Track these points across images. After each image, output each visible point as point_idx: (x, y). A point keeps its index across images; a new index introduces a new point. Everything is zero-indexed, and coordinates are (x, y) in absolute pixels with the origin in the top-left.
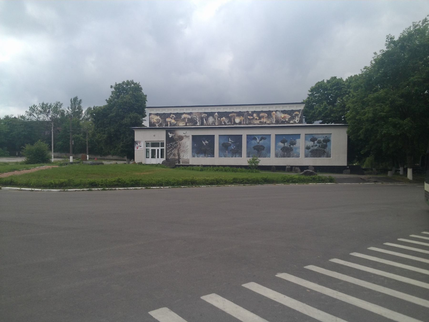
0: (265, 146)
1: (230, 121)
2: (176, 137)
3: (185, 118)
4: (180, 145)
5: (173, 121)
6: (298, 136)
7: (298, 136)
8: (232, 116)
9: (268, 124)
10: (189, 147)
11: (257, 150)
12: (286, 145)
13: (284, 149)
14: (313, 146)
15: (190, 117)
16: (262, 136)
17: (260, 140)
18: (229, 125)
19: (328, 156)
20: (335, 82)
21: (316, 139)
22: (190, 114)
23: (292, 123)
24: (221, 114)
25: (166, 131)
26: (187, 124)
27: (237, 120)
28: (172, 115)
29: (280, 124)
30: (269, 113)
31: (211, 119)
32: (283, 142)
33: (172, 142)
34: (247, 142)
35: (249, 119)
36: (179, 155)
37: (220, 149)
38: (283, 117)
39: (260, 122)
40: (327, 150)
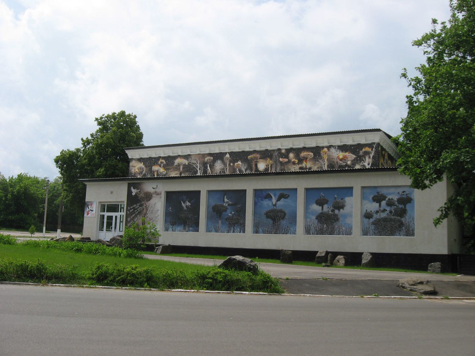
0: (286, 211)
1: (250, 167)
2: (142, 195)
3: (179, 165)
6: (349, 190)
7: (349, 190)
8: (252, 159)
10: (159, 212)
13: (322, 218)
14: (377, 212)
15: (186, 162)
16: (282, 192)
17: (278, 200)
19: (410, 233)
22: (187, 157)
24: (235, 156)
25: (128, 183)
28: (161, 160)
31: (219, 166)
32: (321, 203)
34: (255, 204)
35: (281, 163)
37: (209, 218)
38: (341, 157)
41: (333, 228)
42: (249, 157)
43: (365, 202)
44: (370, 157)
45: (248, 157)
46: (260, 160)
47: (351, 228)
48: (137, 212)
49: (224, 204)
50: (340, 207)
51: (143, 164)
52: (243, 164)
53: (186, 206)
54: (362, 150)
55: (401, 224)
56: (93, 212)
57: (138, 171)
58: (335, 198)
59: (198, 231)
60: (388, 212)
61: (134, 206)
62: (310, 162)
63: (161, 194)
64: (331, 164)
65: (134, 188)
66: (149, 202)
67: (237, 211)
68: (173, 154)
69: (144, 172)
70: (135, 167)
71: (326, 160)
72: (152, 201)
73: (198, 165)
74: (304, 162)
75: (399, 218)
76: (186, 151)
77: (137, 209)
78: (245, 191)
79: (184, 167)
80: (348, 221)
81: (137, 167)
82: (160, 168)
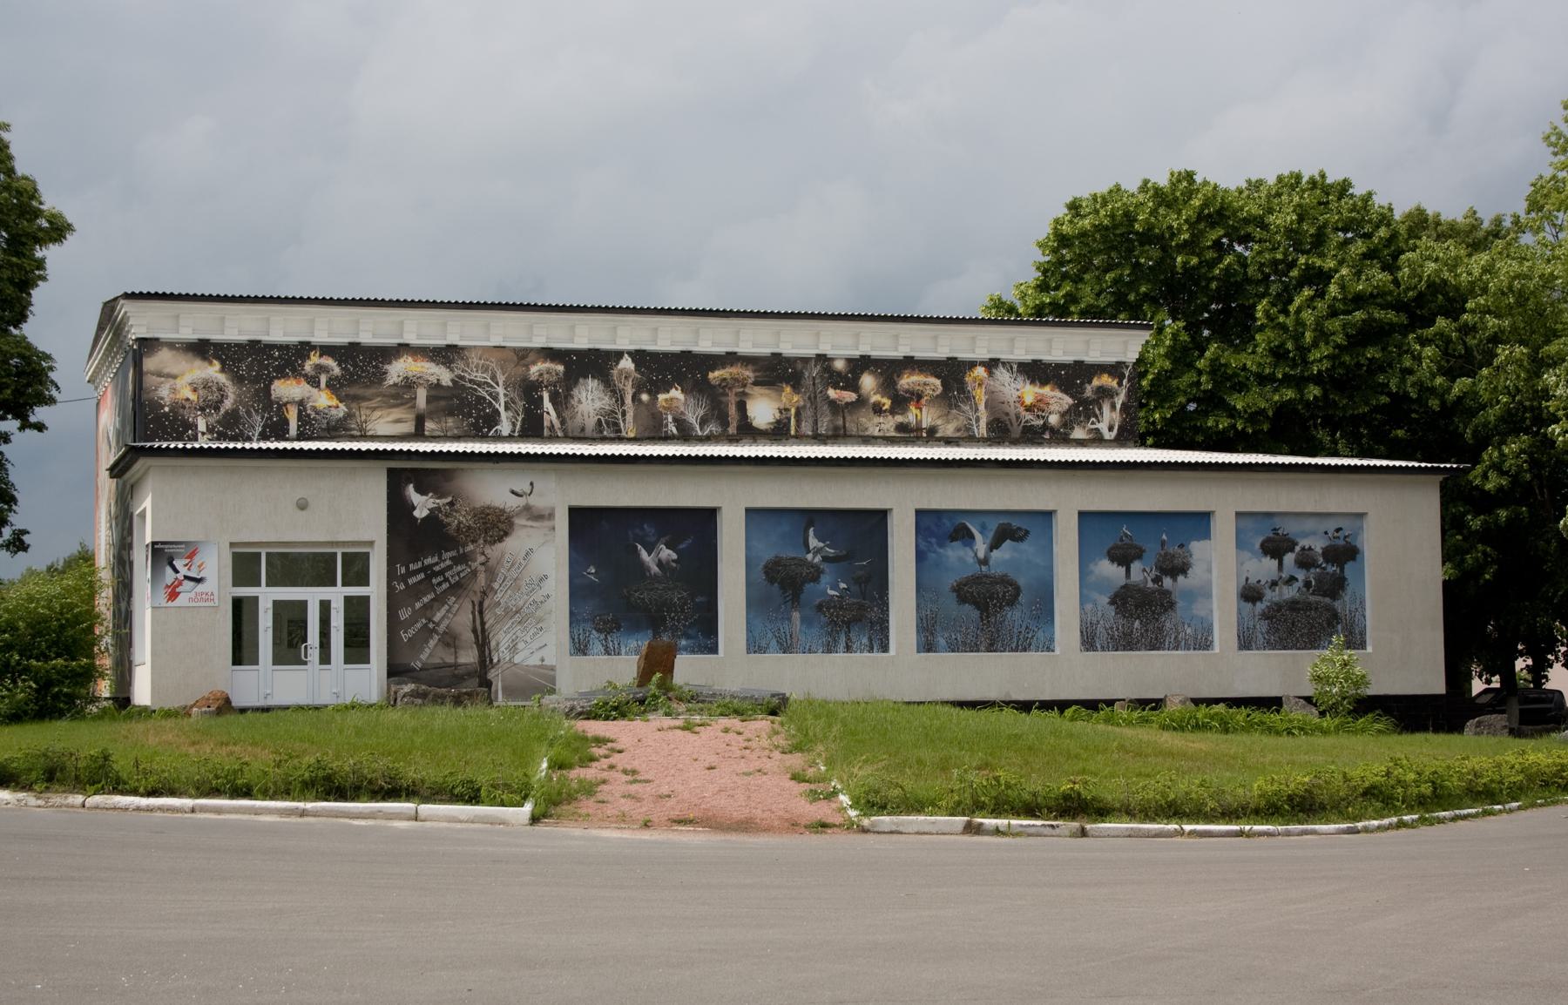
0: (1021, 582)
1: (717, 412)
2: (462, 518)
3: (409, 384)
4: (491, 573)
5: (323, 399)
6: (1199, 522)
7: (1199, 522)
8: (725, 384)
9: (949, 442)
11: (977, 605)
12: (1140, 573)
13: (1125, 599)
14: (1274, 584)
15: (445, 376)
17: (995, 545)
18: (707, 439)
20: (1205, 205)
21: (1291, 546)
22: (446, 354)
23: (1081, 443)
24: (659, 369)
25: (390, 472)
26: (429, 426)
27: (763, 410)
28: (315, 359)
29: (1015, 443)
30: (952, 372)
31: (590, 399)
32: (1123, 557)
33: (435, 544)
34: (920, 556)
35: (833, 405)
36: (483, 641)
37: (756, 603)
38: (1029, 400)
39: (901, 427)
40: (1343, 605)
41: (1161, 630)
42: (714, 376)
43: (1247, 554)
44: (1113, 407)
45: (711, 375)
46: (757, 389)
47: (1210, 630)
48: (445, 586)
49: (809, 557)
50: (1177, 568)
51: (223, 370)
52: (692, 401)
53: (660, 564)
54: (1090, 382)
55: (1334, 618)
56: (200, 588)
57: (193, 397)
58: (1163, 543)
59: (713, 650)
60: (1300, 584)
61: (429, 561)
62: (932, 410)
63: (551, 516)
64: (997, 420)
65: (421, 490)
66: (499, 546)
67: (857, 581)
68: (374, 336)
69: (228, 404)
70: (175, 377)
71: (982, 407)
72: (513, 545)
73: (501, 390)
74: (912, 408)
75: (1327, 600)
77: (442, 572)
78: (881, 516)
79: (433, 393)
80: (1199, 610)
81: (188, 378)
82: (315, 391)
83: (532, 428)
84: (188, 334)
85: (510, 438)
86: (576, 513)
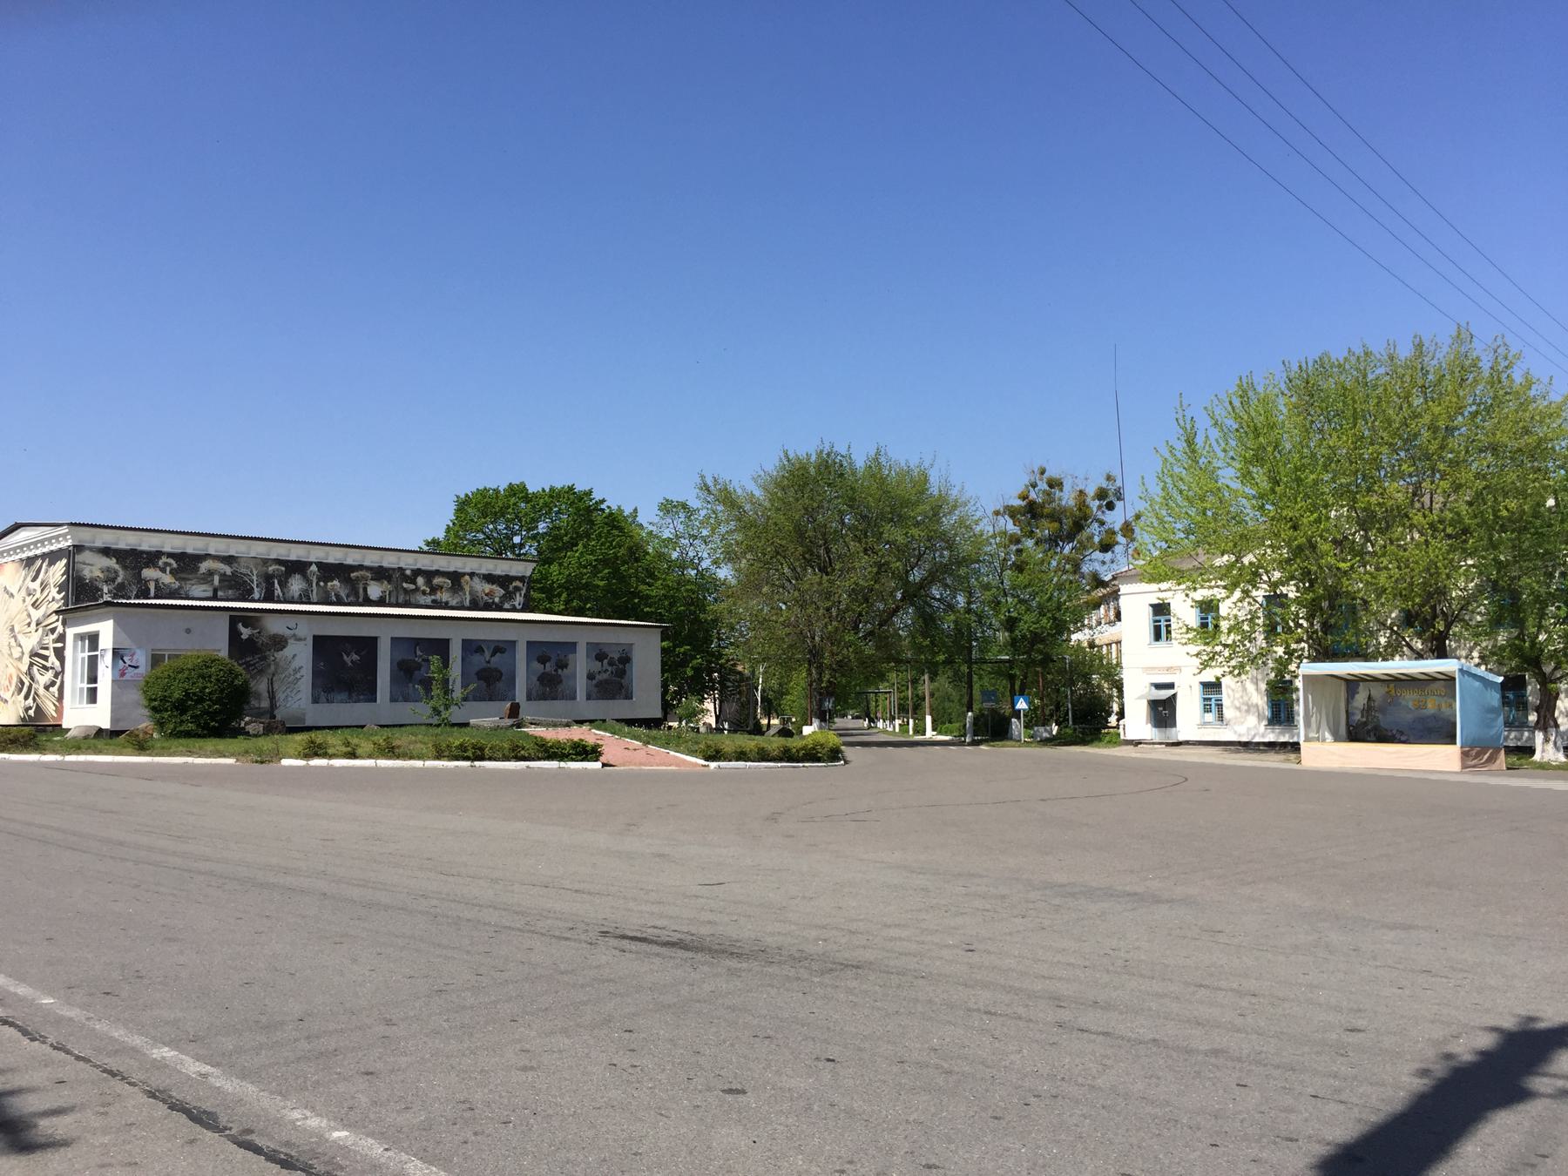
1: (354, 591)
3: (211, 573)
5: (167, 579)
10: (303, 672)
15: (228, 570)
19: (629, 696)
22: (229, 560)
24: (329, 571)
26: (220, 593)
28: (164, 559)
30: (456, 577)
31: (296, 585)
32: (543, 660)
36: (272, 697)
37: (394, 680)
65: (245, 626)
69: (119, 580)
72: (288, 652)
76: (234, 549)
83: (269, 598)
84: (99, 544)
85: (259, 601)
86: (316, 638)
